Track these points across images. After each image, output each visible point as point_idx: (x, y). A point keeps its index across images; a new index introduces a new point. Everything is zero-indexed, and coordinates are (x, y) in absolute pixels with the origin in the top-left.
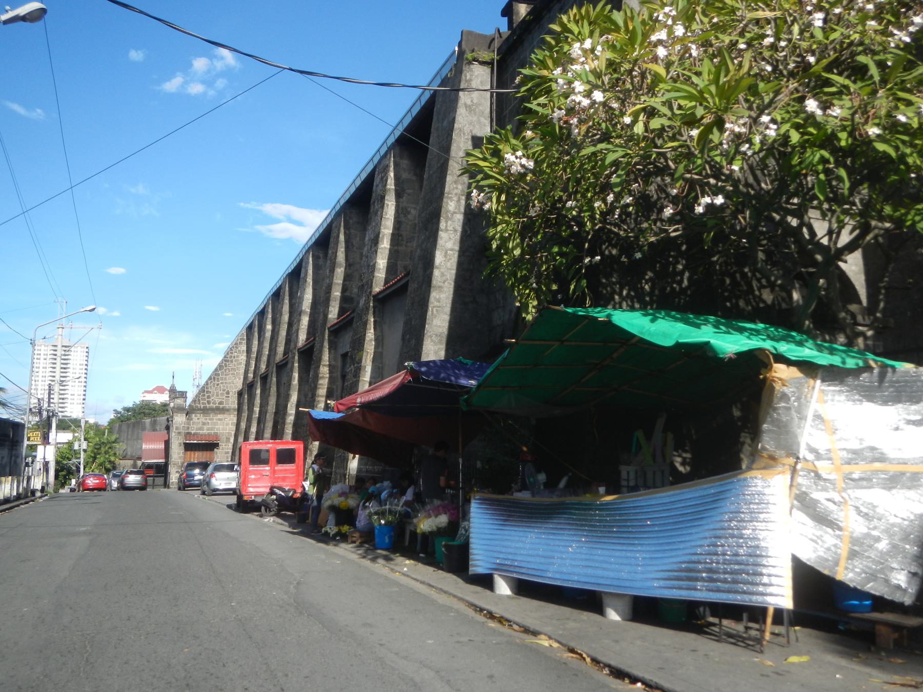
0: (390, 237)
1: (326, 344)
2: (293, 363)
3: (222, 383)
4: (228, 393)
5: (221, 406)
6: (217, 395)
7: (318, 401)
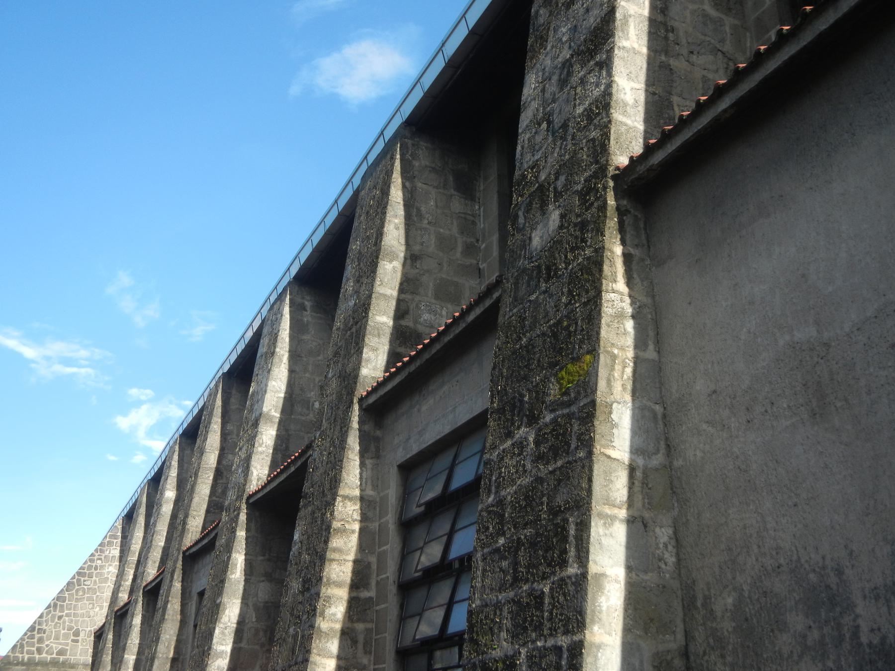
0: (645, 26)
1: (353, 442)
2: (233, 531)
3: (67, 615)
4: (77, 634)
5: (62, 658)
6: (57, 638)
7: (328, 599)
